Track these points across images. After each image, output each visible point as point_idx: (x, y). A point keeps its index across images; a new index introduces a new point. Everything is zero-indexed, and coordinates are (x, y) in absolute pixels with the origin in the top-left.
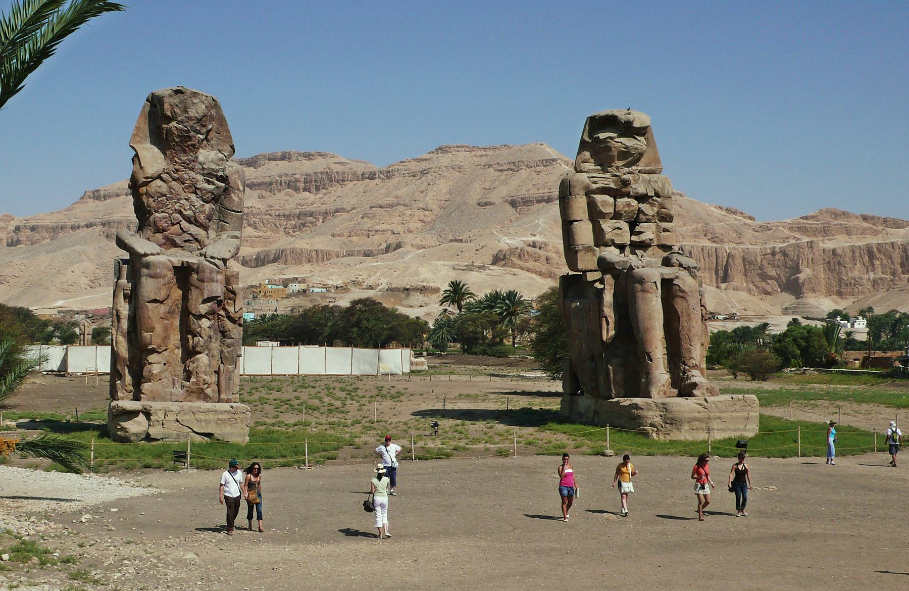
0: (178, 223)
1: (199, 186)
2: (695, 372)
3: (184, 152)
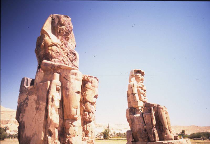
3: (65, 39)
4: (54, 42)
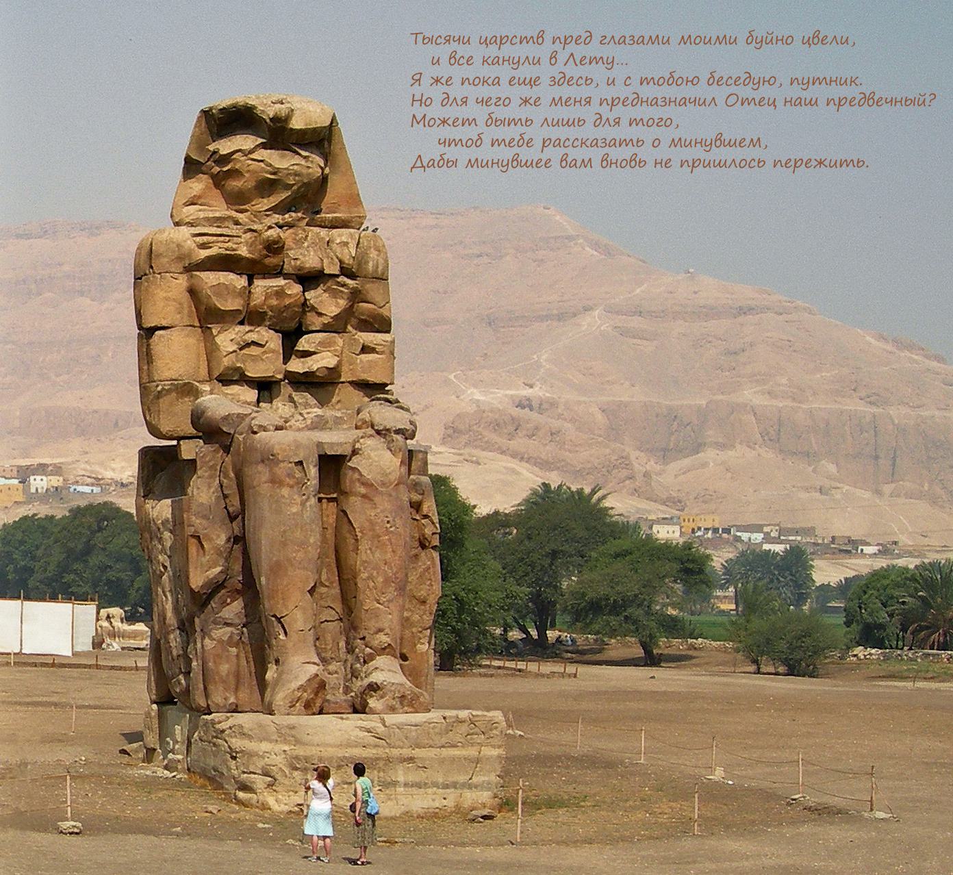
2: (381, 661)
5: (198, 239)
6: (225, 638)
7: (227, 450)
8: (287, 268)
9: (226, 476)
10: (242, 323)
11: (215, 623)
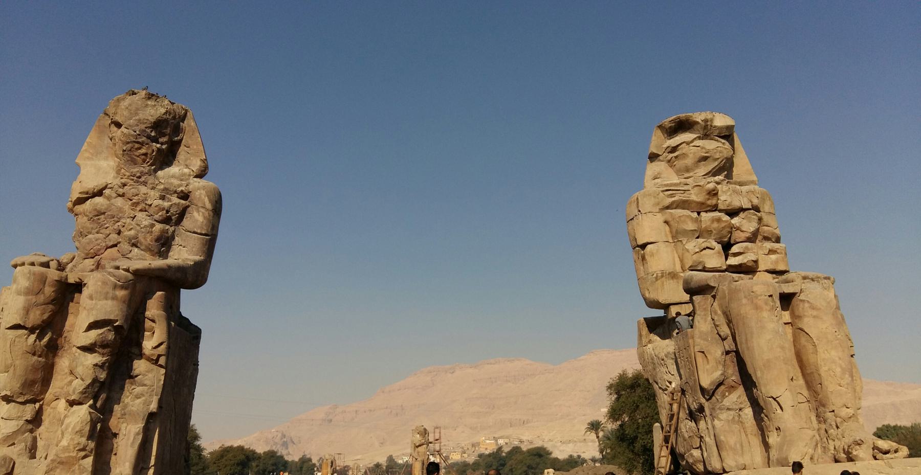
0: (115, 245)
1: (149, 202)
2: (851, 424)
4: (86, 190)
5: (667, 193)
6: (731, 418)
7: (714, 297)
8: (721, 207)
9: (716, 313)
10: (698, 238)
11: (720, 409)
